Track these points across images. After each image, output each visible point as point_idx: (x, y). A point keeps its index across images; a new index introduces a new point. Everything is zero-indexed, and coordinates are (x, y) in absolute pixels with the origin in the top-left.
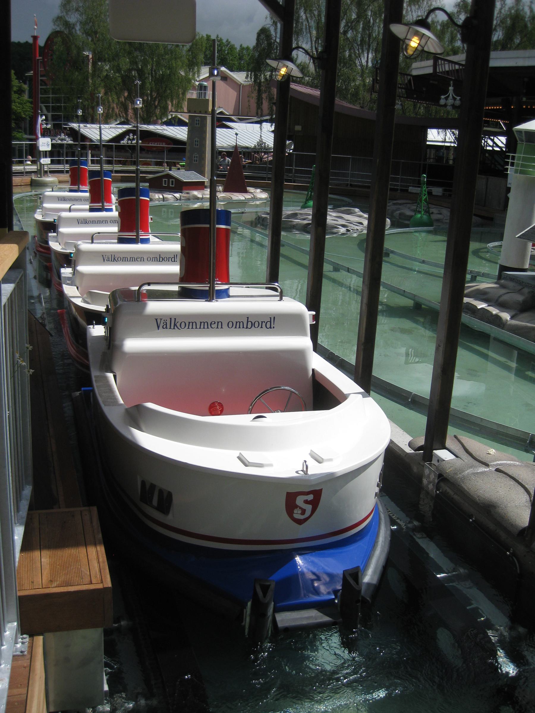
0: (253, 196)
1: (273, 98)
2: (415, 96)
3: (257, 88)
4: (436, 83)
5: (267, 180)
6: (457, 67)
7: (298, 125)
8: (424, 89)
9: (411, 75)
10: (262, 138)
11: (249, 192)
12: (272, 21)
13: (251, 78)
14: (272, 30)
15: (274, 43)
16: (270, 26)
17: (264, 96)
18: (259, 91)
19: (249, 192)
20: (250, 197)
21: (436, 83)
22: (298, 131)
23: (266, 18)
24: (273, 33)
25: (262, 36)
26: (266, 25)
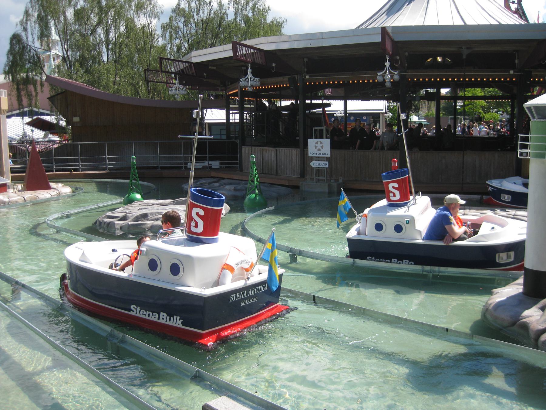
0: (58, 192)
1: (31, 95)
2: (184, 82)
3: (15, 86)
4: (215, 68)
5: (54, 171)
6: (252, 51)
7: (76, 116)
8: (205, 74)
9: (191, 63)
10: (25, 130)
11: (52, 188)
12: (22, 27)
13: (9, 78)
14: (23, 34)
15: (27, 46)
16: (21, 31)
17: (23, 93)
18: (18, 89)
19: (52, 188)
20: (56, 193)
21: (215, 68)
22: (76, 122)
23: (17, 25)
24: (24, 37)
25: (14, 42)
26: (18, 31)
